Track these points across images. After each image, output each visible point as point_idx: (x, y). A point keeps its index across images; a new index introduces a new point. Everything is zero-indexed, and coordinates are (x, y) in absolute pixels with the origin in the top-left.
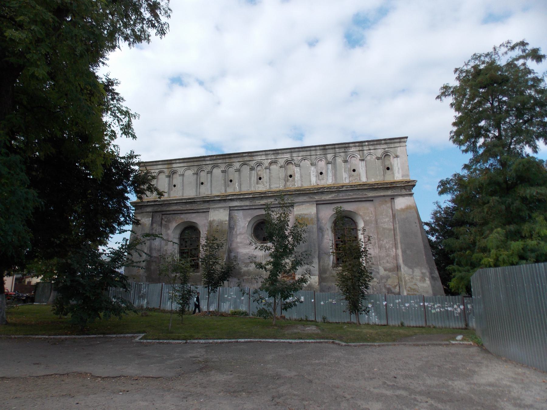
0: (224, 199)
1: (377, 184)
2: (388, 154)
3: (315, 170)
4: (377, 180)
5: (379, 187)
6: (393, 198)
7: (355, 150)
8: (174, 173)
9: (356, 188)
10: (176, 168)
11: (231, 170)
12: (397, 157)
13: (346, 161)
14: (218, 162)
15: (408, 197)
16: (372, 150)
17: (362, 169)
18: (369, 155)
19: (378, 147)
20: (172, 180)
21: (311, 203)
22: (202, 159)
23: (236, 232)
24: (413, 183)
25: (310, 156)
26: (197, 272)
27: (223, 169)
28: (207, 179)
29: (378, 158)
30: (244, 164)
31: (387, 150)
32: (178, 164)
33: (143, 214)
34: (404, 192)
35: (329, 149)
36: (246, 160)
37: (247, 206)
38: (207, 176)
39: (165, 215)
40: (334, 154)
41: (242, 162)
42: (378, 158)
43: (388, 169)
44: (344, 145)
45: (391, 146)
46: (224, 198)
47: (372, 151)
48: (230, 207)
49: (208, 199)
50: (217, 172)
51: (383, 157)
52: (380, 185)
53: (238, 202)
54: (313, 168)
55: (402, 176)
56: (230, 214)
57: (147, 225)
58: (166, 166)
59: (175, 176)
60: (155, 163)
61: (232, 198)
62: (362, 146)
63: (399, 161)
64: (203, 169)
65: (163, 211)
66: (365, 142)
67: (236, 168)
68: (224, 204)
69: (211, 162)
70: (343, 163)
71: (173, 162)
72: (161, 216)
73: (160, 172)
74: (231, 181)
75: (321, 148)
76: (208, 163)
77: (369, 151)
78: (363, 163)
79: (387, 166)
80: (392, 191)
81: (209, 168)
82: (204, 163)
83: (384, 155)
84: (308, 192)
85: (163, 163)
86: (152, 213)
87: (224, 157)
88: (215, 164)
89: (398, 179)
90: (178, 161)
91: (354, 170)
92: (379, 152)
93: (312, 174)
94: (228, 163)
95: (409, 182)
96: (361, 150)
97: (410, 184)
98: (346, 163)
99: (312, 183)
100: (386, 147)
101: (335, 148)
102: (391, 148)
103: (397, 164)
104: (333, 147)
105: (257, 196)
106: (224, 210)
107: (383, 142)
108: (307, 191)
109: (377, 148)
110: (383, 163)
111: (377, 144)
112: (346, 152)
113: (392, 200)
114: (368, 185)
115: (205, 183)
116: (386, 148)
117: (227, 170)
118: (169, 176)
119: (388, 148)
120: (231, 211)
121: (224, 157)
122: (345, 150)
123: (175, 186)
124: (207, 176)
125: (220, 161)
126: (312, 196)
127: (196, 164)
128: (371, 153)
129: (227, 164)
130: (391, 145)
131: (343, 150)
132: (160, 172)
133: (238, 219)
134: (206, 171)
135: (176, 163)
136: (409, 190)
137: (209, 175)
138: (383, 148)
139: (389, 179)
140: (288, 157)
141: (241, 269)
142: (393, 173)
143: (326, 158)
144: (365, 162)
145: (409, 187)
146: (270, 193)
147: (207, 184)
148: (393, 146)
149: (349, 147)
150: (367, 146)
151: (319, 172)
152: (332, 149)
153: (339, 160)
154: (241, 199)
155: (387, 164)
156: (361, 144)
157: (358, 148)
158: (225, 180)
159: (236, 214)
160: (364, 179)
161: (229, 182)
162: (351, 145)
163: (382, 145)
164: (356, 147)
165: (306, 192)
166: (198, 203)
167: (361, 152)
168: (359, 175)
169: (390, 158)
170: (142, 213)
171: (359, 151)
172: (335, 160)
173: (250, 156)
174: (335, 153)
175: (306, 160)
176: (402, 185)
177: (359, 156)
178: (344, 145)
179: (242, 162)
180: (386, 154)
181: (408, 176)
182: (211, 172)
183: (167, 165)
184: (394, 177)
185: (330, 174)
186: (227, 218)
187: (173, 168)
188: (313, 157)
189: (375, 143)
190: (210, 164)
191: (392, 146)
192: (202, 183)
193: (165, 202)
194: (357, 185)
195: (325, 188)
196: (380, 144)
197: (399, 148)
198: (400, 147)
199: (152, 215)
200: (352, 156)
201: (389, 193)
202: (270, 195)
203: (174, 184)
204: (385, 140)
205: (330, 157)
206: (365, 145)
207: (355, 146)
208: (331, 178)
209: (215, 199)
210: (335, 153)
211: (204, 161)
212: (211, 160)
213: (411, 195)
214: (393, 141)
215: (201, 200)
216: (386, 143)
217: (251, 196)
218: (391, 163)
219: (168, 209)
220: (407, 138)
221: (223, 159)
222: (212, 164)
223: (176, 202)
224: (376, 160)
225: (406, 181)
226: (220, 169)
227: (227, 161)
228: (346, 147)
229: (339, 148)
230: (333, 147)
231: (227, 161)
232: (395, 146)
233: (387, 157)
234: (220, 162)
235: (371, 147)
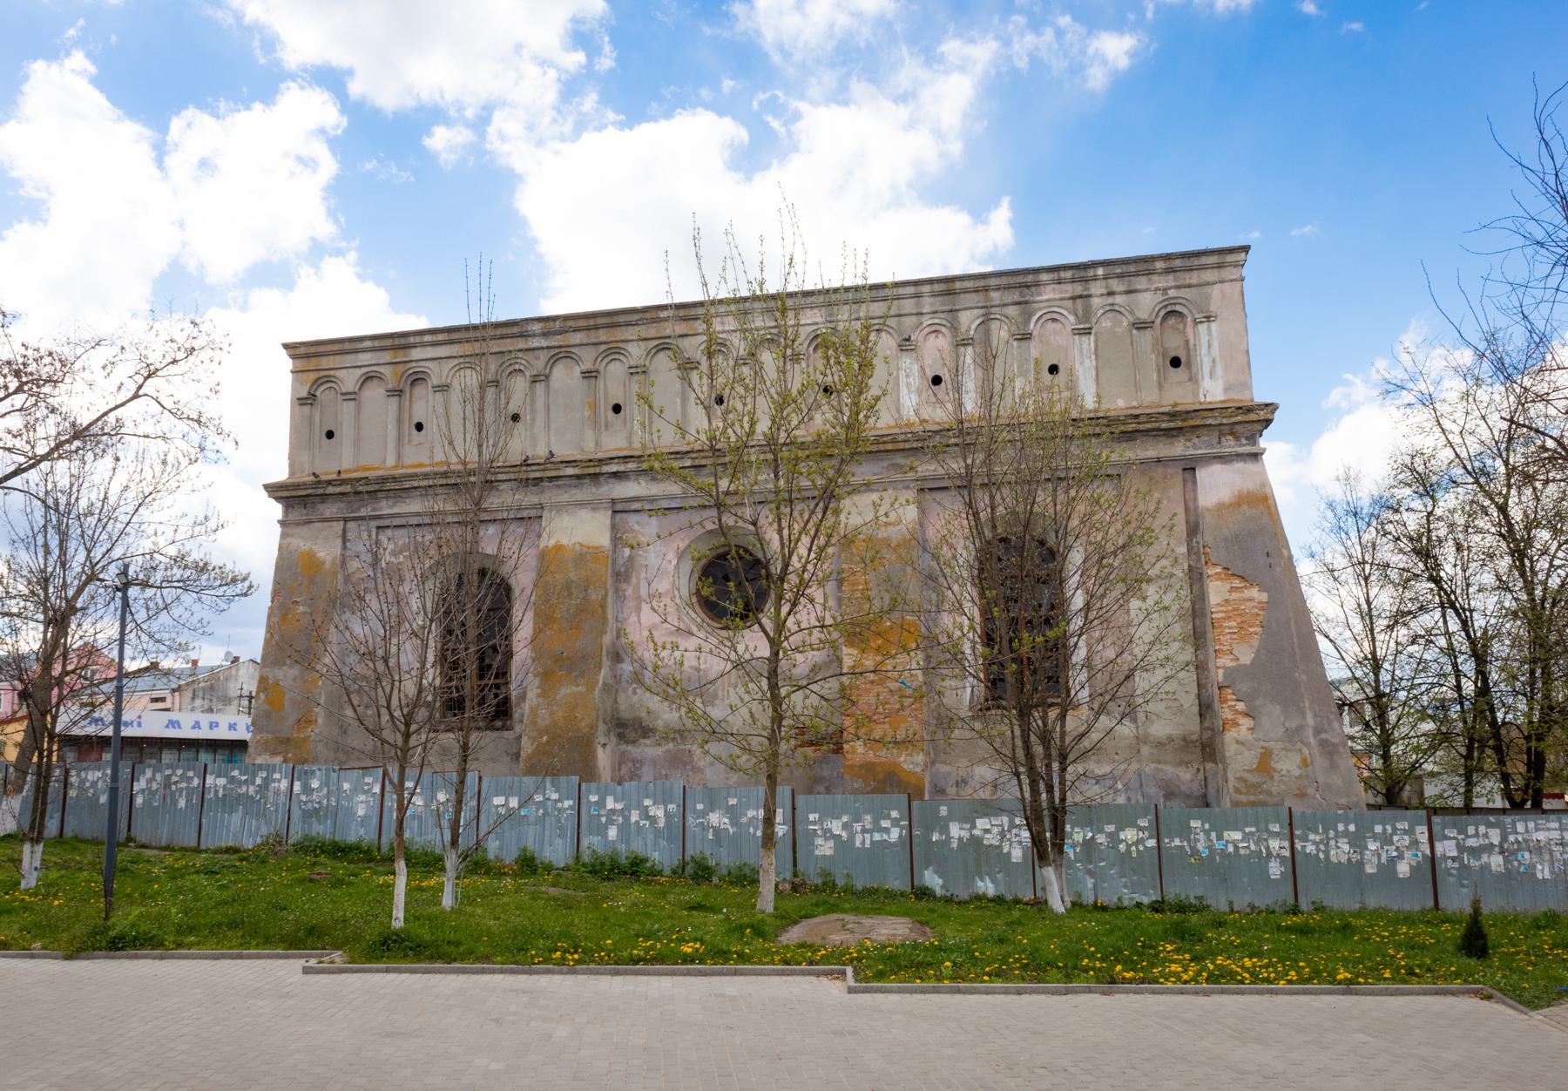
0: (592, 472)
1: (1137, 416)
2: (1178, 308)
3: (916, 368)
4: (1135, 404)
5: (1142, 427)
6: (1189, 468)
7: (1057, 297)
8: (418, 379)
10: (421, 364)
11: (616, 370)
12: (1208, 318)
14: (572, 342)
15: (1245, 461)
16: (1120, 293)
18: (1110, 315)
19: (1142, 282)
20: (411, 405)
21: (900, 486)
22: (515, 330)
23: (637, 588)
24: (1262, 415)
25: (896, 319)
26: (503, 728)
27: (587, 366)
28: (533, 401)
29: (1141, 326)
31: (1172, 293)
32: (429, 348)
33: (312, 525)
34: (1230, 445)
35: (966, 291)
36: (668, 332)
37: (672, 498)
38: (532, 390)
39: (389, 532)
40: (982, 311)
41: (657, 342)
42: (1141, 326)
43: (1176, 362)
44: (1020, 279)
45: (1188, 281)
46: (592, 471)
47: (1119, 299)
48: (613, 501)
49: (538, 475)
50: (565, 377)
51: (1158, 321)
52: (1144, 423)
53: (643, 482)
54: (907, 361)
55: (1226, 390)
56: (613, 527)
57: (327, 565)
58: (387, 357)
59: (419, 390)
60: (347, 346)
61: (622, 468)
62: (1085, 280)
63: (1214, 334)
64: (517, 367)
65: (380, 517)
67: (632, 363)
68: (594, 490)
69: (544, 343)
70: (1015, 343)
71: (412, 340)
72: (374, 531)
73: (368, 378)
74: (617, 409)
75: (937, 287)
76: (535, 343)
77: (1110, 300)
78: (1088, 343)
79: (1173, 354)
80: (1188, 444)
81: (539, 362)
82: (521, 344)
83: (1163, 313)
84: (889, 447)
85: (377, 343)
86: (342, 523)
87: (591, 322)
88: (561, 347)
89: (1208, 400)
90: (427, 338)
91: (1053, 369)
92: (1147, 303)
93: (903, 381)
94: (605, 343)
95: (1249, 410)
96: (1081, 297)
97: (1253, 417)
98: (1023, 343)
99: (904, 412)
100: (1172, 283)
102: (1190, 286)
103: (1209, 346)
104: (980, 283)
106: (594, 509)
107: (1159, 265)
108: (884, 443)
109: (1139, 287)
110: (1158, 344)
111: (1137, 274)
112: (1026, 303)
113: (1188, 475)
114: (1105, 421)
115: (526, 417)
116: (1171, 288)
117: (601, 370)
118: (397, 393)
119: (1178, 287)
120: (618, 517)
121: (591, 322)
122: (1022, 295)
123: (419, 427)
124: (532, 390)
125: (578, 338)
126: (902, 461)
127: (495, 346)
128: (1117, 308)
129: (603, 347)
130: (1187, 275)
131: (1016, 297)
132: (368, 378)
134: (528, 374)
135: (423, 345)
136: (1247, 439)
137: (540, 388)
138: (1157, 289)
139: (1177, 394)
140: (817, 320)
141: (656, 719)
142: (1193, 380)
143: (954, 328)
145: (1249, 426)
147: (533, 419)
148: (1194, 281)
149: (1037, 284)
150: (1104, 283)
151: (930, 375)
152: (977, 291)
153: (1000, 333)
154: (649, 474)
155: (1174, 346)
156: (1083, 274)
157: (1069, 287)
158: (594, 406)
159: (636, 527)
160: (1090, 402)
161: (611, 413)
162: (1044, 277)
163: (1155, 277)
165: (881, 447)
166: (503, 486)
167: (1079, 301)
168: (1072, 385)
169: (1185, 326)
170: (310, 522)
171: (1073, 298)
172: (987, 333)
173: (685, 319)
174: (986, 307)
175: (883, 335)
176: (1225, 421)
177: (1072, 318)
178: (1020, 279)
179: (657, 342)
180: (1169, 309)
181: (1247, 386)
182: (547, 377)
183: (391, 352)
184: (1196, 393)
185: (970, 383)
186: (604, 540)
187: (414, 364)
188: (909, 321)
189: (1132, 268)
190: (542, 348)
191: (1194, 278)
192: (516, 418)
195: (951, 433)
196: (1150, 273)
197: (1217, 287)
198: (1222, 282)
199: (344, 531)
200: (1048, 316)
201: (1179, 448)
203: (416, 421)
204: (1167, 257)
205: (969, 320)
206: (1095, 278)
207: (1059, 282)
208: (972, 395)
209: (561, 473)
210: (986, 307)
211: (523, 335)
212: (545, 335)
213: (1256, 456)
214: (1196, 262)
215: (512, 476)
216: (1170, 271)
217: (688, 463)
218: (1187, 342)
219: (396, 510)
220: (1246, 249)
221: (588, 329)
222: (548, 348)
223: (425, 483)
224: (1134, 331)
225: (1240, 405)
226: (577, 367)
227: (603, 338)
229: (998, 289)
230: (980, 283)
231: (603, 335)
232: (1201, 281)
233: (1172, 321)
234: (578, 341)
235: (1116, 285)
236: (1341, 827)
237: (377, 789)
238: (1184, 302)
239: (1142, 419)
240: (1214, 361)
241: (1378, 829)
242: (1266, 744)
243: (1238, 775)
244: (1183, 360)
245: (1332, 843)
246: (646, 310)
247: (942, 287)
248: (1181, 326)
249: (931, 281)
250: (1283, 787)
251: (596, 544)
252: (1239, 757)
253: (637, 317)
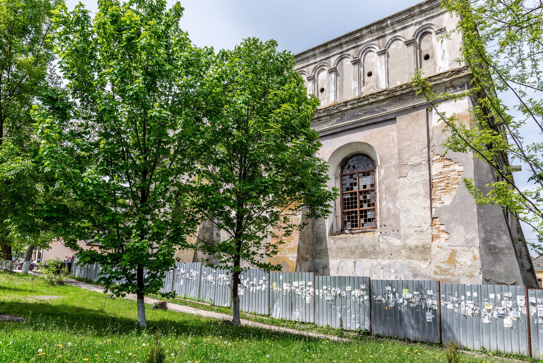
9: (366, 102)
13: (356, 62)
17: (381, 68)
29: (408, 43)
31: (424, 23)
35: (333, 48)
44: (352, 37)
47: (398, 34)
55: (450, 65)
62: (383, 29)
66: (385, 20)
75: (322, 49)
91: (370, 74)
101: (341, 45)
107: (417, 10)
111: (406, 19)
114: (385, 92)
119: (427, 19)
136: (460, 87)
142: (435, 64)
144: (386, 55)
145: (461, 80)
150: (391, 27)
151: (320, 88)
152: (337, 46)
153: (347, 62)
157: (376, 34)
162: (364, 32)
164: (373, 34)
168: (377, 80)
169: (431, 38)
176: (446, 80)
177: (377, 48)
180: (424, 31)
184: (435, 70)
194: (368, 96)
196: (412, 17)
206: (387, 26)
207: (371, 32)
216: (422, 12)
228: (358, 38)
229: (347, 42)
233: (425, 38)
236: (468, 294)
238: (428, 26)
239: (404, 87)
240: (444, 51)
241: (492, 296)
242: (454, 248)
243: (436, 265)
244: (430, 55)
245: (463, 303)
247: (322, 49)
248: (430, 39)
249: (318, 47)
250: (461, 271)
252: (439, 255)
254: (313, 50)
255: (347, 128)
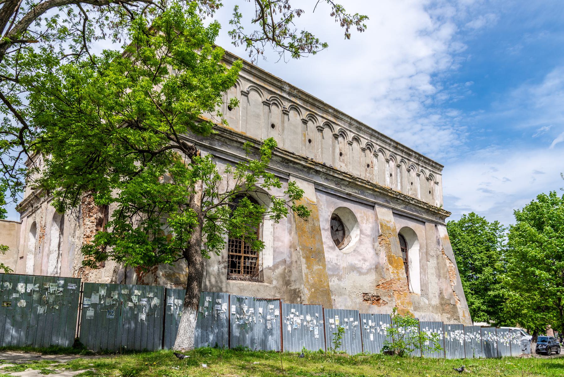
27: (304, 117)
30: (328, 124)
99: (386, 183)
105: (347, 179)
133: (321, 206)
146: (360, 180)
193: (227, 135)
202: (359, 183)
212: (289, 94)
237: (277, 312)
246: (325, 105)
251: (312, 200)
253: (321, 106)
254: (391, 140)
255: (408, 215)
